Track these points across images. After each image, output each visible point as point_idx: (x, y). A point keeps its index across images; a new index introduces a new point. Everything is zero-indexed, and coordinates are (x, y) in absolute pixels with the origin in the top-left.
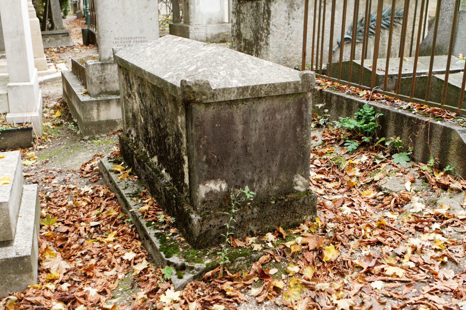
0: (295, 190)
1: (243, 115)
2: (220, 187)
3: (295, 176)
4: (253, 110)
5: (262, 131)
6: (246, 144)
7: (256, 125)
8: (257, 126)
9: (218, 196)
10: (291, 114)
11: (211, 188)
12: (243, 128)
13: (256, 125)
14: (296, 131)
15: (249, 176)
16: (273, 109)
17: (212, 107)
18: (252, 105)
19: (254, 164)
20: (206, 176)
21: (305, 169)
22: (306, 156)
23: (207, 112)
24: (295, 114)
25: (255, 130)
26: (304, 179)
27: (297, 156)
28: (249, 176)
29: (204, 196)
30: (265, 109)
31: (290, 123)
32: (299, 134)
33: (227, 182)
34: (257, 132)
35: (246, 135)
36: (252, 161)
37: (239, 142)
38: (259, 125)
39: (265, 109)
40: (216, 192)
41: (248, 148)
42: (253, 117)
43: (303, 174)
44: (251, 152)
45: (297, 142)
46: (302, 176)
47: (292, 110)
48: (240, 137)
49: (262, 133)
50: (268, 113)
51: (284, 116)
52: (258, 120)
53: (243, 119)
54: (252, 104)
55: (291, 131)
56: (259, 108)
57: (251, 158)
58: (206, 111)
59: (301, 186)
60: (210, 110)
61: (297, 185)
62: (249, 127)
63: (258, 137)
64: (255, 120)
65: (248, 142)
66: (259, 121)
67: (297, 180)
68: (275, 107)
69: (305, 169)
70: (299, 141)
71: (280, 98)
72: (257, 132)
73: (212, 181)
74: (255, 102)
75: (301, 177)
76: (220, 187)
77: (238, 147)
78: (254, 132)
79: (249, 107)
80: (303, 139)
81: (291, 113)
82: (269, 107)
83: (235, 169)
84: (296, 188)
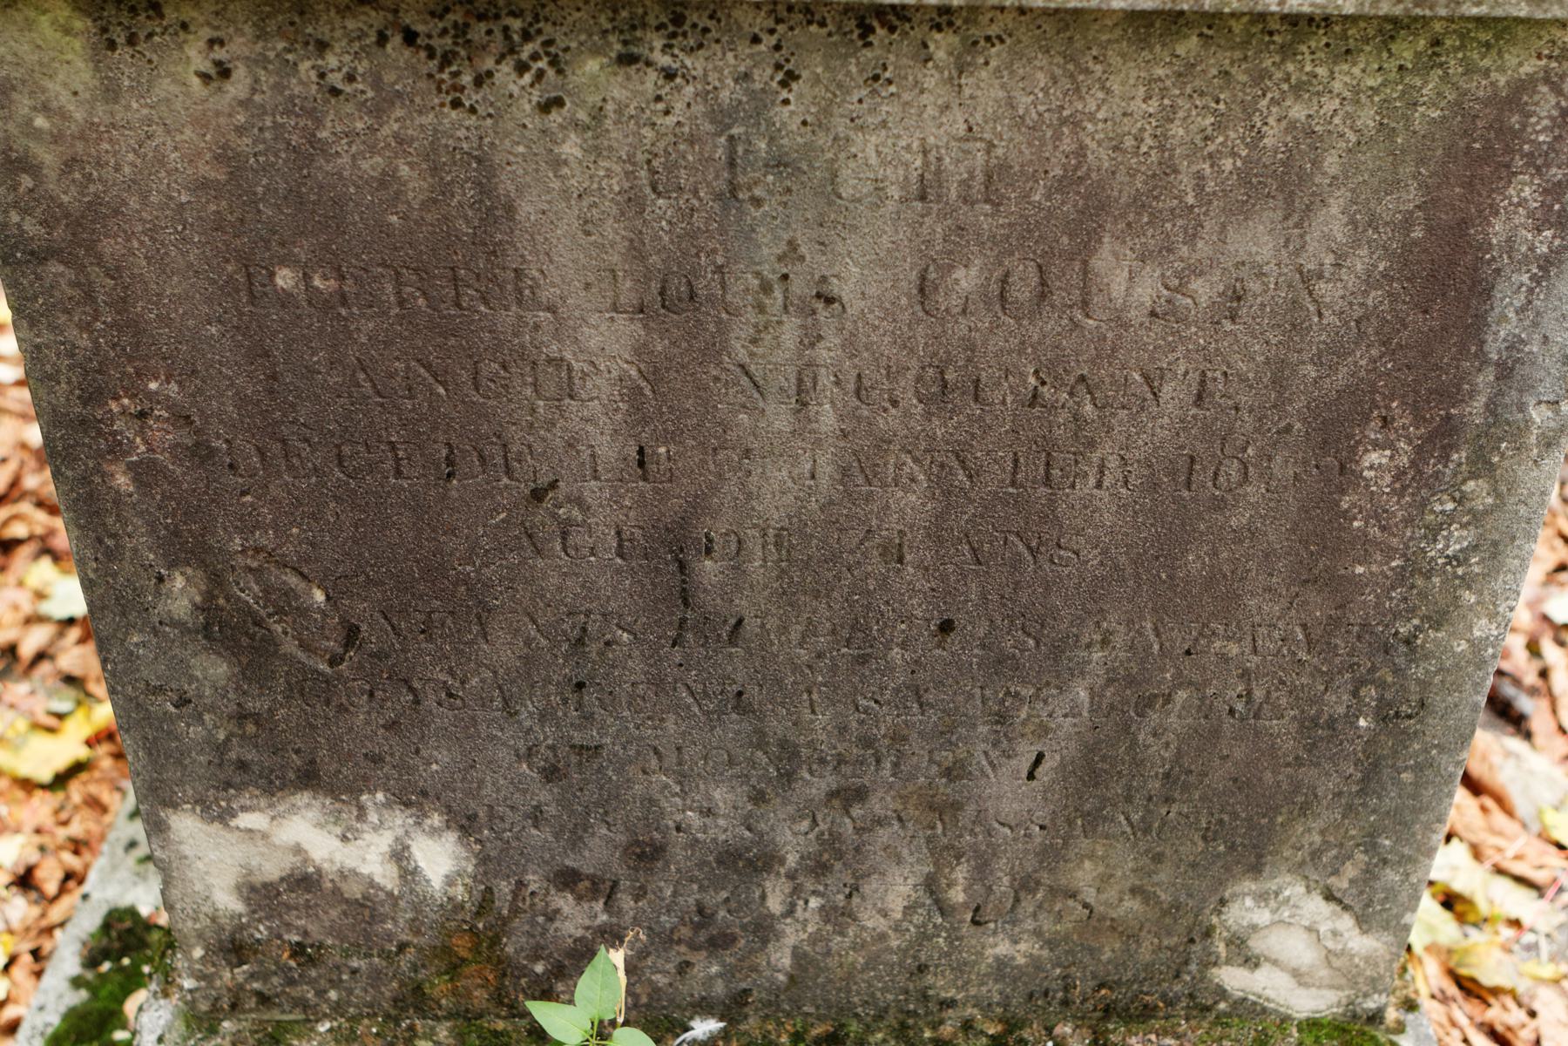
0: (1222, 993)
1: (633, 203)
2: (400, 855)
3: (1248, 885)
4: (779, 163)
5: (889, 421)
6: (684, 522)
7: (812, 339)
8: (823, 353)
9: (376, 918)
10: (1308, 279)
11: (298, 850)
12: (641, 350)
13: (812, 339)
14: (1346, 472)
15: (708, 812)
16: (1063, 185)
17: (196, 57)
18: (759, 105)
19: (777, 726)
20: (222, 748)
21: (1371, 846)
22: (1407, 737)
23: (136, 109)
24: (1370, 281)
25: (802, 397)
26: (1346, 922)
27: (1308, 725)
28: (708, 812)
29: (228, 902)
30: (955, 172)
31: (1280, 376)
32: (1378, 515)
33: (465, 825)
34: (827, 418)
35: (668, 437)
36: (753, 692)
37: (592, 490)
38: (850, 346)
39: (955, 172)
40: (354, 890)
41: (709, 569)
42: (768, 250)
43: (1340, 884)
44: (742, 604)
45: (1340, 588)
46: (1329, 896)
47: (1332, 221)
48: (608, 447)
49: (883, 443)
50: (983, 217)
51: (1204, 290)
52: (845, 290)
53: (636, 251)
54: (764, 76)
55: (1283, 467)
56: (868, 146)
57: (737, 666)
58: (111, 92)
59: (1296, 974)
60: (165, 87)
61: (1252, 962)
62: (715, 350)
63: (826, 470)
64: (799, 287)
65: (698, 506)
66: (855, 307)
67: (1263, 917)
68: (1098, 156)
69: (1371, 846)
70: (1357, 584)
71: (1189, 46)
72: (827, 418)
73: (303, 798)
74: (813, 66)
75: (1316, 907)
76: (400, 855)
77: (578, 538)
78: (780, 418)
79: (721, 118)
80: (1414, 568)
81: (1316, 255)
82: (1012, 146)
83: (547, 735)
84: (1233, 978)
